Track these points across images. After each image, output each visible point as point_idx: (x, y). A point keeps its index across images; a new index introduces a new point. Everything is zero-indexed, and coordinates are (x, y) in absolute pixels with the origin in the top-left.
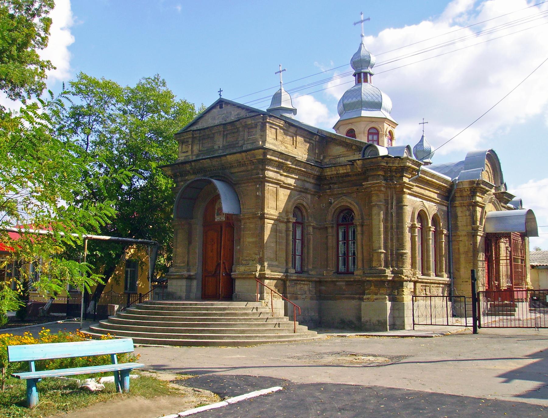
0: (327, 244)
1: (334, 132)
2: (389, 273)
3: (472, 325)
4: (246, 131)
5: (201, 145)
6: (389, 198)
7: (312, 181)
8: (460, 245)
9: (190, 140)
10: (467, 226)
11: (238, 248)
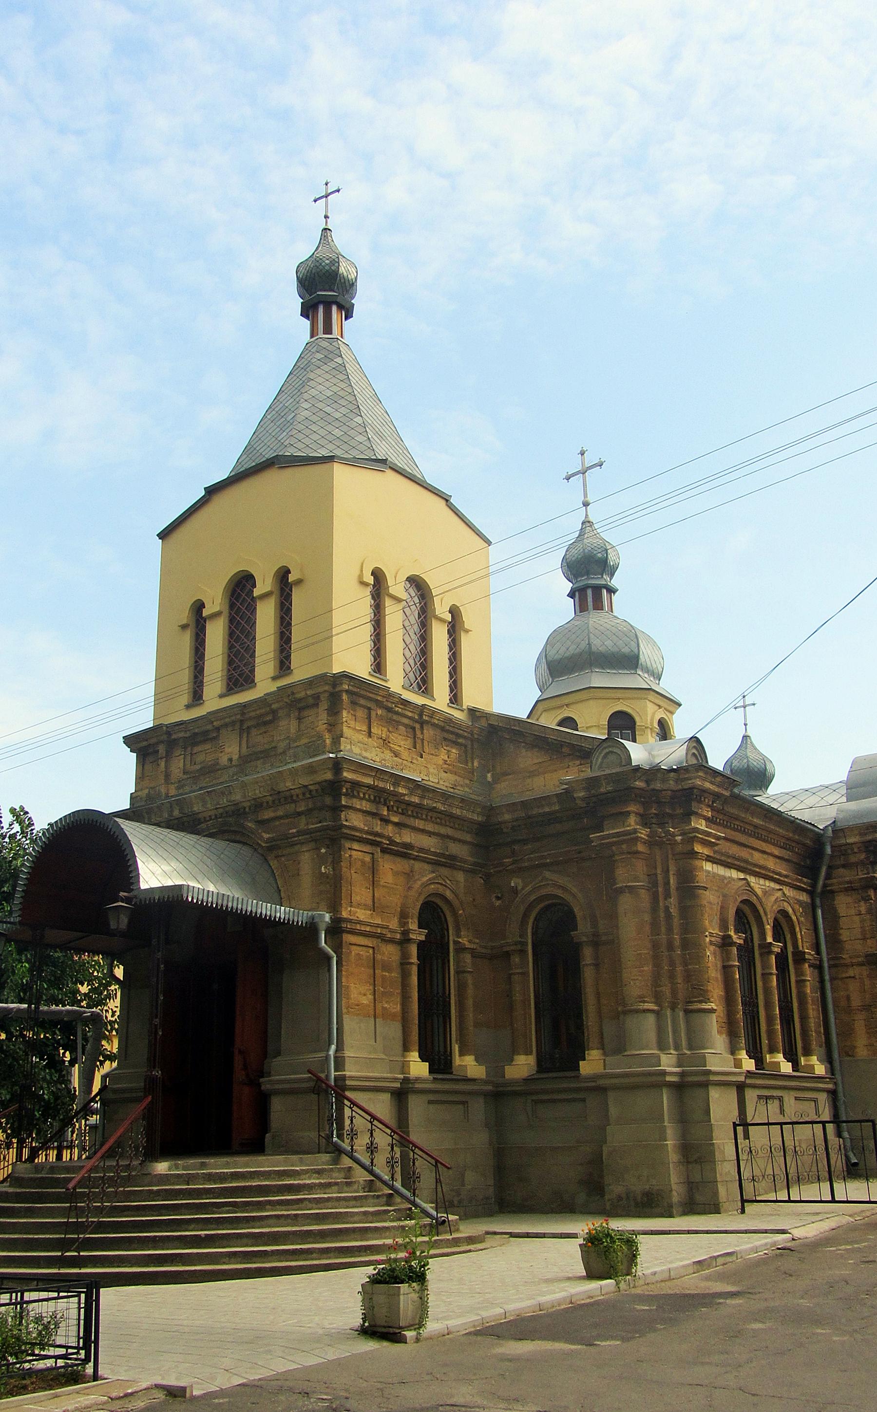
4: (294, 714)
5: (189, 758)
6: (659, 871)
7: (468, 838)
8: (851, 988)
9: (162, 749)
10: (864, 939)
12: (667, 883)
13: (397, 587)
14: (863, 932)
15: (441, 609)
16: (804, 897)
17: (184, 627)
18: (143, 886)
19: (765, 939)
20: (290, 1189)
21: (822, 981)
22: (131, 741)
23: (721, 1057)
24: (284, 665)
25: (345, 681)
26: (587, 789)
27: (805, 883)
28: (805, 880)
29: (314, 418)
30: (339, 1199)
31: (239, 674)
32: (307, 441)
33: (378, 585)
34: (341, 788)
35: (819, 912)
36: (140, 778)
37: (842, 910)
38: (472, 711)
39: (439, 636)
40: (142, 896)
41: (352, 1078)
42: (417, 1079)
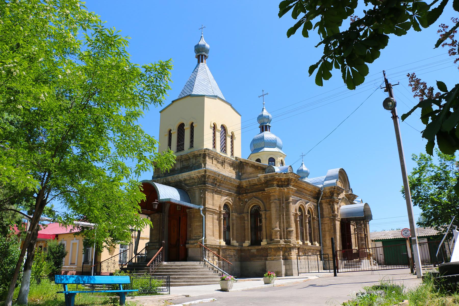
0: (244, 226)
2: (282, 242)
12: (283, 200)
13: (219, 128)
16: (315, 204)
18: (161, 198)
20: (195, 268)
21: (319, 224)
23: (295, 241)
24: (192, 146)
25: (207, 151)
26: (265, 178)
27: (315, 200)
31: (180, 147)
32: (197, 90)
33: (214, 128)
38: (236, 158)
39: (229, 140)
41: (208, 245)
42: (223, 246)
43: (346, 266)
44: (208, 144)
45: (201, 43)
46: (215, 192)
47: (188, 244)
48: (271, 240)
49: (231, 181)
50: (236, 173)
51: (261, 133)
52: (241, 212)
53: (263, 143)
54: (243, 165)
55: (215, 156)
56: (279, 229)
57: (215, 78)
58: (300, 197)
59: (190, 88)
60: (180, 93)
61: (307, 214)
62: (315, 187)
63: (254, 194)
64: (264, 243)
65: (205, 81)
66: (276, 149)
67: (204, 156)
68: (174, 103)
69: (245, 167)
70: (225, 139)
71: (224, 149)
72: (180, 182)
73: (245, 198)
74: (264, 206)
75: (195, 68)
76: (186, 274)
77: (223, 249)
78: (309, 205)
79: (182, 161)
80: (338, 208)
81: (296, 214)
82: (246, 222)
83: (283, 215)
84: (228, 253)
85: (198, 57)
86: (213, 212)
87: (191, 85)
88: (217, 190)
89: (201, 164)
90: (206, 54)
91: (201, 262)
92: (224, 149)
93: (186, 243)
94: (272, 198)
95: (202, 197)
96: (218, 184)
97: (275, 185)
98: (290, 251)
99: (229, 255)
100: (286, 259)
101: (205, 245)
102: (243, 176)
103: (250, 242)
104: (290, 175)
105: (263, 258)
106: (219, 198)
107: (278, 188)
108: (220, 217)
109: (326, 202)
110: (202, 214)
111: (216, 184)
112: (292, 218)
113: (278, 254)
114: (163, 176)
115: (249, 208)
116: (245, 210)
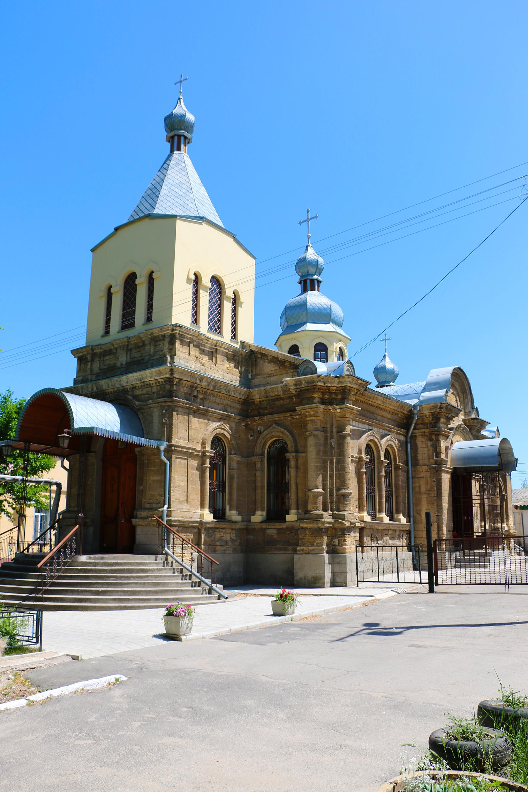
0: (255, 482)
1: (275, 349)
2: (327, 518)
3: (427, 581)
5: (102, 362)
6: (328, 426)
8: (421, 482)
10: (429, 459)
11: (141, 488)
12: (332, 432)
13: (206, 281)
14: (429, 455)
15: (229, 293)
16: (402, 438)
17: (101, 297)
18: (76, 426)
19: (380, 458)
21: (408, 478)
22: (74, 352)
23: (355, 514)
24: (149, 319)
25: (178, 329)
26: (296, 385)
28: (403, 430)
29: (169, 194)
30: (165, 576)
31: (128, 321)
32: (165, 206)
33: (197, 281)
34: (173, 381)
35: (409, 445)
36: (79, 371)
37: (420, 445)
38: (242, 343)
39: (227, 307)
40: (75, 431)
41: (174, 521)
43: (459, 564)
44: (181, 315)
45: (178, 111)
46: (194, 412)
47: (136, 517)
48: (305, 512)
49: (229, 391)
50: (241, 373)
51: (302, 293)
52: (247, 453)
53: (304, 314)
54: (256, 358)
55: (195, 339)
56: (321, 491)
57: (205, 183)
58: (369, 425)
59: (150, 201)
60: (131, 212)
61: (382, 458)
62: (403, 405)
63: (276, 417)
64: (292, 517)
65: (184, 186)
66: (330, 327)
67: (172, 339)
68: (119, 232)
69: (261, 362)
70: (220, 306)
71: (216, 326)
72: (124, 391)
73: (259, 425)
74: (295, 441)
75: (165, 163)
76: (121, 584)
77: (207, 529)
78: (387, 441)
79: (131, 349)
80: (447, 448)
81: (360, 459)
82: (258, 473)
83: (331, 463)
84: (218, 536)
85: (171, 140)
86: (189, 454)
87: (153, 196)
88: (198, 409)
89: (165, 356)
90: (186, 134)
91: (159, 556)
92: (216, 326)
93: (133, 516)
94: (310, 426)
95: (165, 424)
96: (201, 396)
97: (316, 400)
98: (344, 535)
99: (220, 540)
100: (335, 551)
101: (167, 521)
102: (256, 381)
103: (264, 513)
104: (347, 380)
105: (290, 547)
106: (203, 426)
107: (322, 407)
108: (203, 463)
109: (424, 435)
110: (163, 458)
111: (196, 397)
112: (351, 468)
113: (318, 541)
114: (94, 378)
115: (264, 445)
116: (258, 450)
